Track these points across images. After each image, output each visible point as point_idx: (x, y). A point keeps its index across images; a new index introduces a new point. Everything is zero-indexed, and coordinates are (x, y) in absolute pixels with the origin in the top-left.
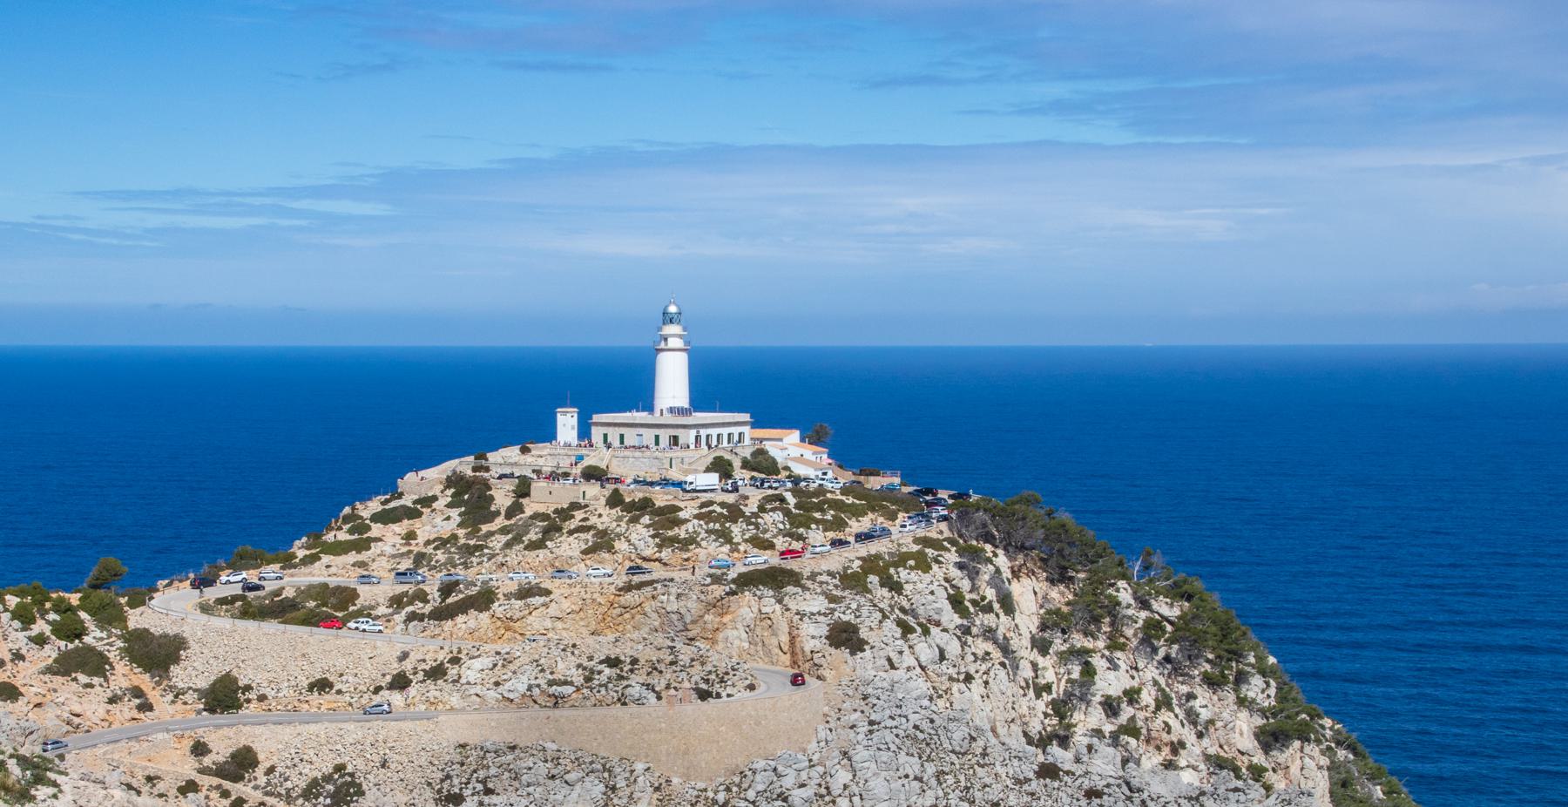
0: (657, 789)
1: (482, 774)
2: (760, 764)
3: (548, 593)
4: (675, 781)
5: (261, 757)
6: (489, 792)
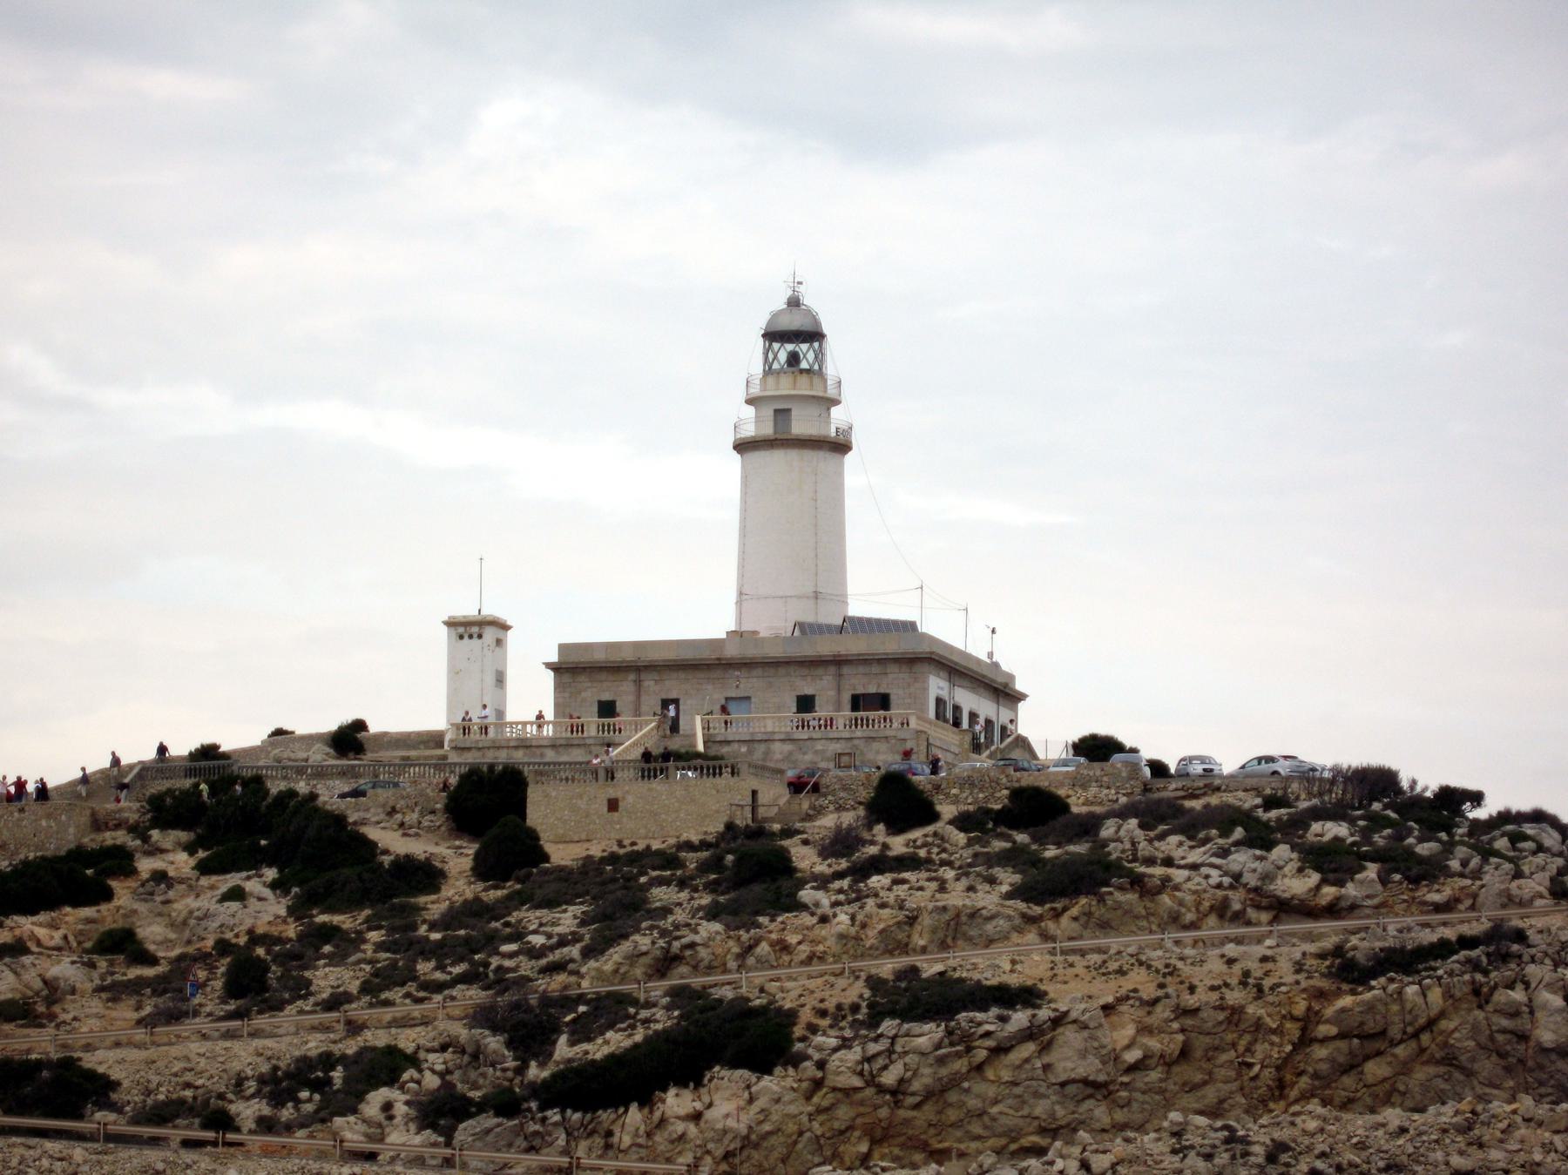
3: (1028, 996)
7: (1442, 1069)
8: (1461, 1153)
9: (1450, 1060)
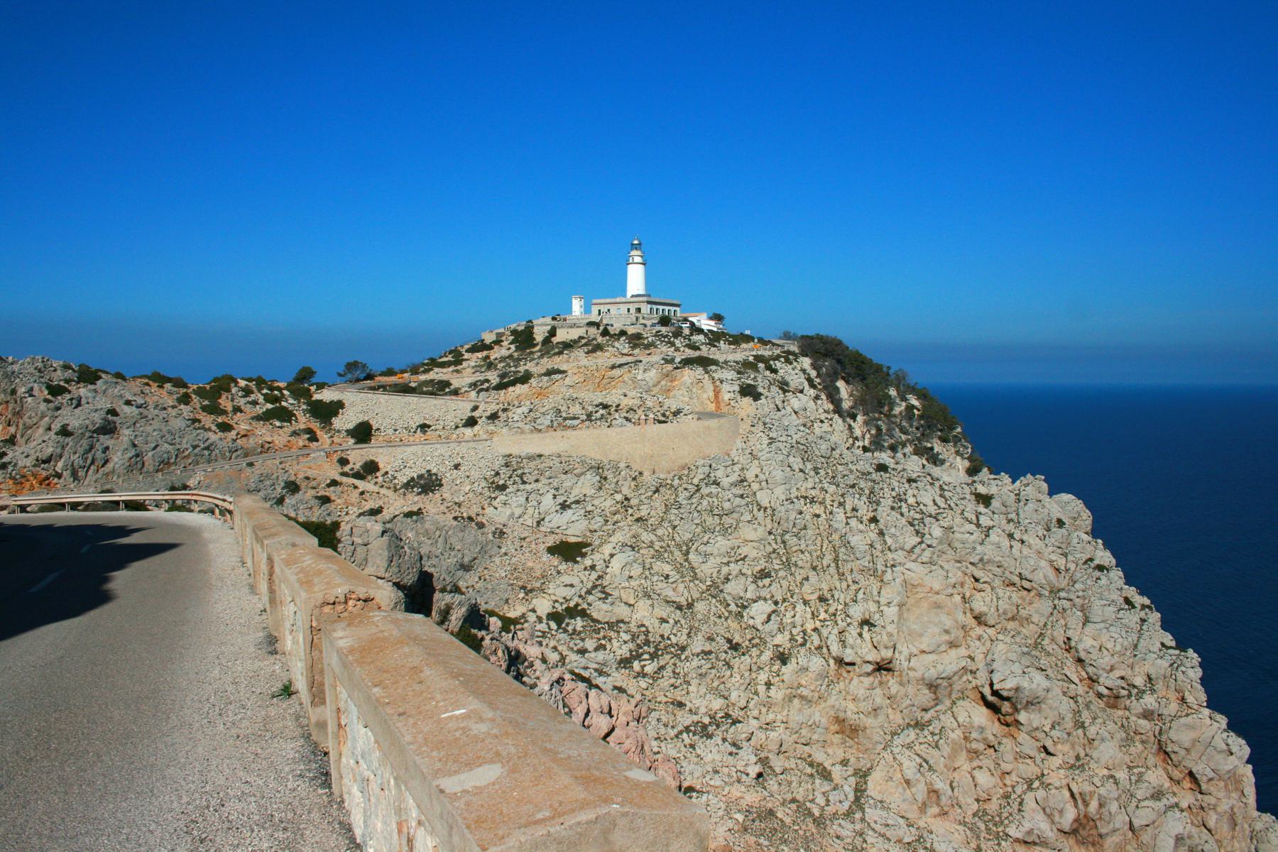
0: (634, 479)
1: (520, 472)
2: (701, 462)
4: (646, 473)
5: (381, 465)
6: (524, 483)
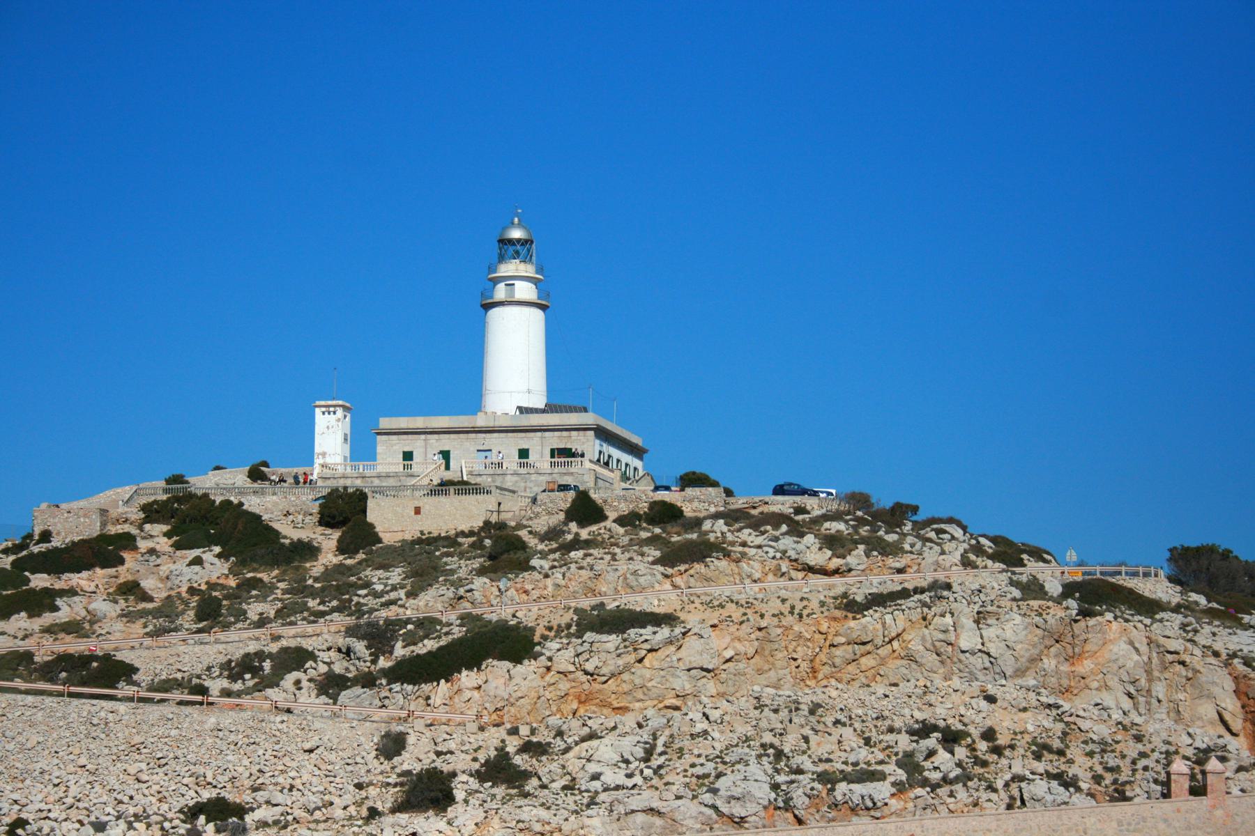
7: (905, 662)
8: (919, 709)
9: (911, 658)
